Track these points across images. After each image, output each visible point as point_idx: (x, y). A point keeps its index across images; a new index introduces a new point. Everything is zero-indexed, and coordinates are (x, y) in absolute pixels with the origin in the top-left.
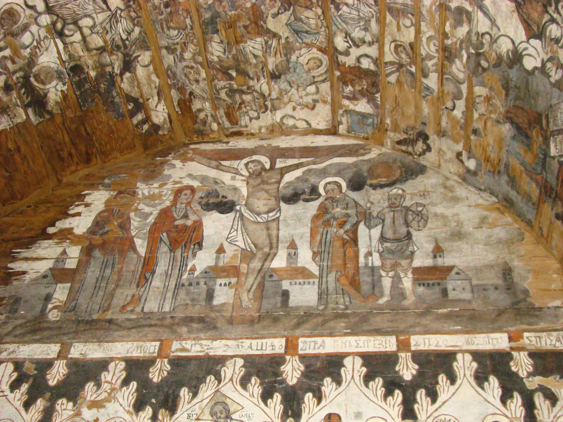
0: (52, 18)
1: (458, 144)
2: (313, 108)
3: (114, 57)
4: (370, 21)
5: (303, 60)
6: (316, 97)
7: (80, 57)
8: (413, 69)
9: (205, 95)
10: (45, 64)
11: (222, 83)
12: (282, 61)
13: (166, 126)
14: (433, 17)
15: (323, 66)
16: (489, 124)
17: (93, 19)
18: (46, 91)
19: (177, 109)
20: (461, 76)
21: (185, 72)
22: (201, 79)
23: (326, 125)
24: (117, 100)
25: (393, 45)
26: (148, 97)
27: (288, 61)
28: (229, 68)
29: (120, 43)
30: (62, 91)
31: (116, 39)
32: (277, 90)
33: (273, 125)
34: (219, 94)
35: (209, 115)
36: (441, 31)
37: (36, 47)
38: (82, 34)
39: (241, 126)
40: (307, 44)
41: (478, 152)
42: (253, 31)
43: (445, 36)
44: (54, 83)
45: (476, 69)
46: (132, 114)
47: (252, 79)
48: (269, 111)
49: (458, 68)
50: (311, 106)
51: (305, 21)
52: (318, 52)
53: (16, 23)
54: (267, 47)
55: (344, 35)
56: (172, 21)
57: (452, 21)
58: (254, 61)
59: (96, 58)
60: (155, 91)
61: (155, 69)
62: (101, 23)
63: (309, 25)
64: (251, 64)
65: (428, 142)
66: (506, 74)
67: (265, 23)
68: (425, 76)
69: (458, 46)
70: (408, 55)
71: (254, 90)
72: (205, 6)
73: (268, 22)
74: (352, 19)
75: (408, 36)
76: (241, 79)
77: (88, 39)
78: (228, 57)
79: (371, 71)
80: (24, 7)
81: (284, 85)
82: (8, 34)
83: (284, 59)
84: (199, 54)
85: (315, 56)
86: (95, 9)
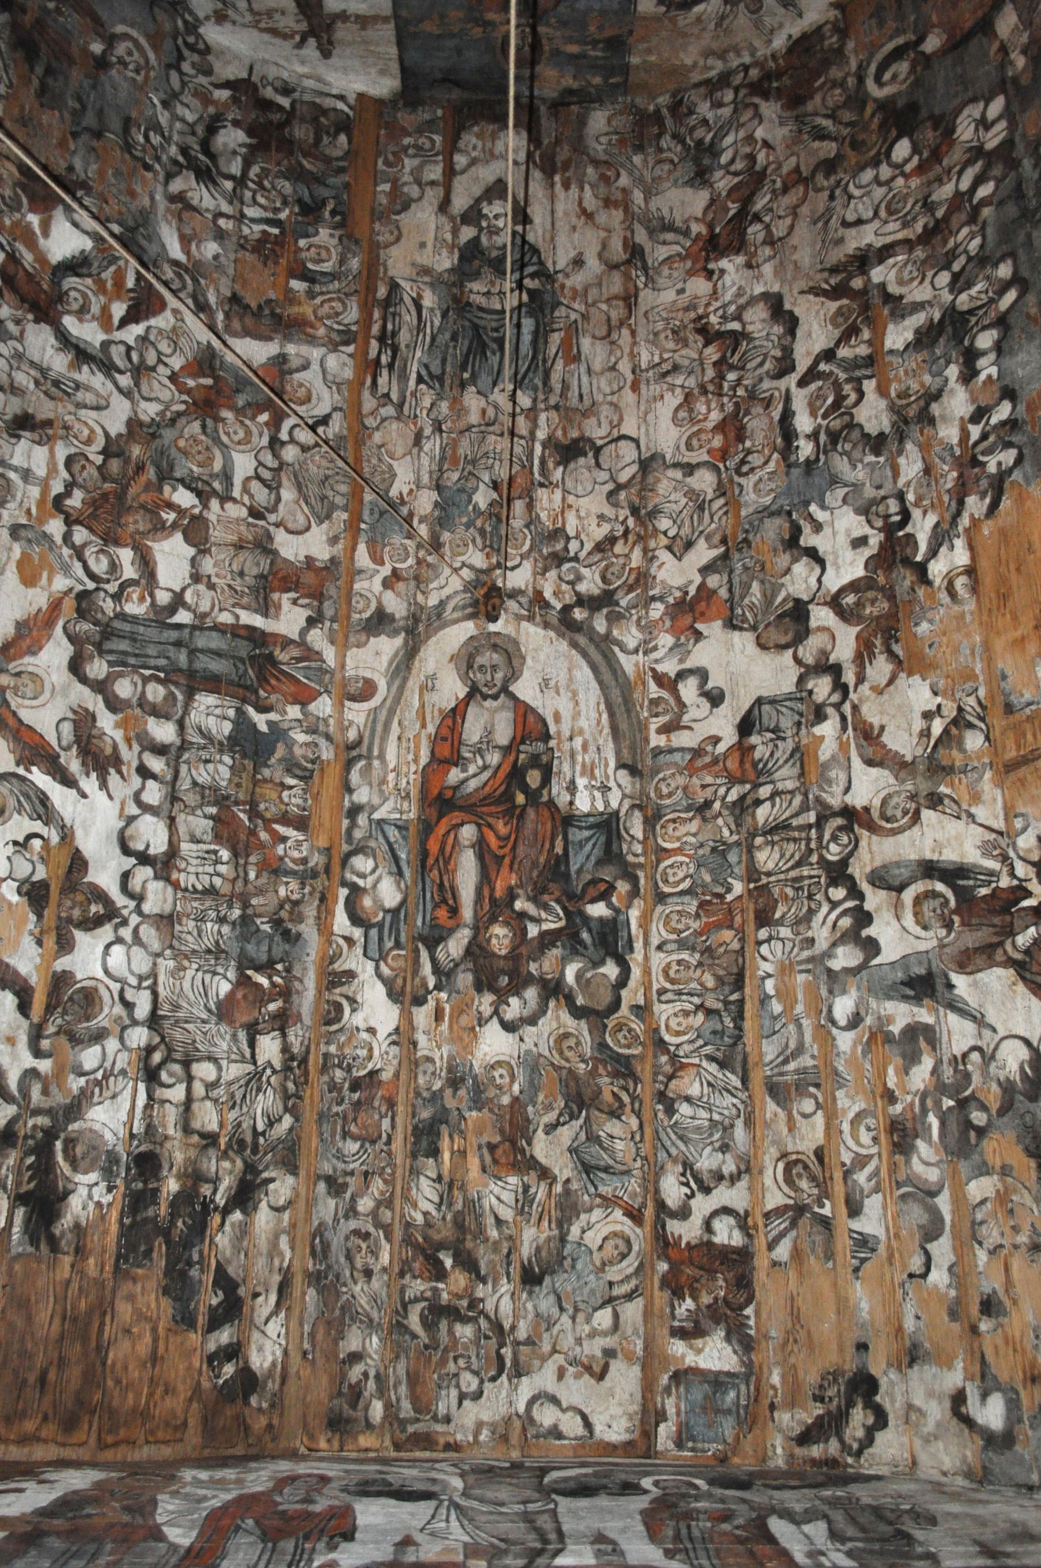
0: (151, 1039)
1: (950, 1367)
2: (601, 1377)
3: (226, 1164)
4: (732, 1126)
5: (593, 1239)
6: (609, 1342)
7: (166, 1137)
8: (827, 1211)
9: (375, 1315)
10: (97, 1127)
11: (418, 1286)
12: (549, 1239)
13: (270, 1384)
14: (859, 1069)
15: (633, 1254)
16: (1016, 1265)
17: (220, 1069)
18: (71, 1186)
19: (306, 1346)
20: (933, 1175)
21: (350, 1244)
22: (377, 1268)
23: (628, 1430)
24: (194, 1272)
25: (781, 1166)
26: (258, 1289)
27: (563, 1239)
28: (441, 1246)
29: (249, 1139)
30: (99, 1204)
31: (244, 1125)
32: (530, 1316)
33: (508, 1421)
34: (406, 1317)
35: (372, 1373)
36: (879, 1090)
37: (98, 1083)
38: (189, 1090)
39: (435, 1418)
40: (603, 1198)
41: (1003, 1368)
42: (503, 1160)
43: (890, 1097)
44: (93, 1177)
45: (964, 1141)
46: (214, 1324)
47: (484, 1280)
48: (504, 1377)
49: (926, 1160)
50: (597, 1369)
51: (607, 1142)
52: (625, 1219)
53: (88, 1019)
54: (524, 1202)
55: (680, 1169)
56: (355, 1120)
57: (899, 1061)
58: (493, 1233)
59: (192, 1153)
60: (277, 1278)
61: (293, 1225)
62: (230, 1084)
63: (610, 1151)
64: (487, 1240)
65: (878, 1399)
66: (1028, 1118)
67: (529, 1144)
68: (854, 1210)
69: (917, 1110)
70: (813, 1178)
71: (482, 1312)
72: (425, 1094)
73: (535, 1141)
74: (698, 1129)
75: (811, 1134)
76: (459, 1280)
77: (195, 1106)
78: (444, 1218)
79: (736, 1251)
80: (116, 997)
81: (546, 1304)
82: (66, 1033)
83: (556, 1232)
84: (389, 1203)
85: (618, 1228)
86: (230, 1051)
